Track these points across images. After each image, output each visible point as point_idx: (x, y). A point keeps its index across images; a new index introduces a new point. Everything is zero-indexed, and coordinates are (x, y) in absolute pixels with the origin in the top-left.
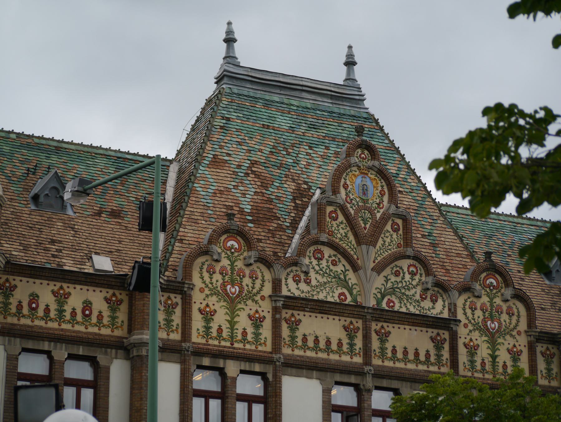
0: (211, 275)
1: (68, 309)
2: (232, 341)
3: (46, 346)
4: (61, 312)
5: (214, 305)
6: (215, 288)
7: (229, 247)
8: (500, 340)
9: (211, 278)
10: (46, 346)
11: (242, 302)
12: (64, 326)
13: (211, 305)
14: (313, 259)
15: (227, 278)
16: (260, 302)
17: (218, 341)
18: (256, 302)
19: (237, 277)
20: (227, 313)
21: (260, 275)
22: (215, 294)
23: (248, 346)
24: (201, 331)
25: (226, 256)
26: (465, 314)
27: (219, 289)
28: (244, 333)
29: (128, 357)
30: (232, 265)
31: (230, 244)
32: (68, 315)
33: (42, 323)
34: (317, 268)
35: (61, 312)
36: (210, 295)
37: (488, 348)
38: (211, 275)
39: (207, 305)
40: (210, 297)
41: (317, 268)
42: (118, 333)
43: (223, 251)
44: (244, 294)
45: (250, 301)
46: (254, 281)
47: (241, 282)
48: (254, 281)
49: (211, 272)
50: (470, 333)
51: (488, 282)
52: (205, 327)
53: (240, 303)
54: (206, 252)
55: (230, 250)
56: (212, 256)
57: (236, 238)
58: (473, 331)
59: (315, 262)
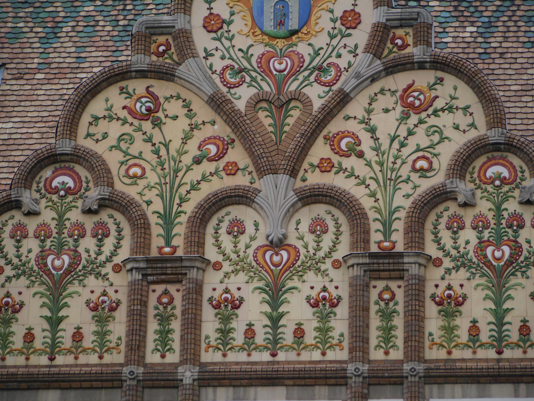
0: (18, 241)
2: (500, 345)
5: (239, 289)
6: (463, 256)
7: (491, 177)
8: (518, 279)
9: (18, 248)
11: (519, 274)
15: (486, 234)
16: (112, 276)
17: (470, 350)
18: (105, 277)
19: (507, 230)
22: (464, 265)
24: (212, 339)
25: (50, 204)
26: (438, 241)
27: (471, 254)
28: (78, 336)
30: (498, 209)
31: (491, 172)
32: (239, 338)
36: (454, 268)
37: (264, 301)
38: (455, 233)
39: (449, 288)
40: (233, 275)
43: (479, 187)
44: (522, 258)
45: (92, 278)
46: (100, 240)
47: (516, 237)
48: (100, 240)
50: (447, 276)
51: (489, 173)
52: (443, 328)
53: (513, 274)
55: (492, 183)
56: (456, 199)
57: (72, 169)
58: (454, 272)
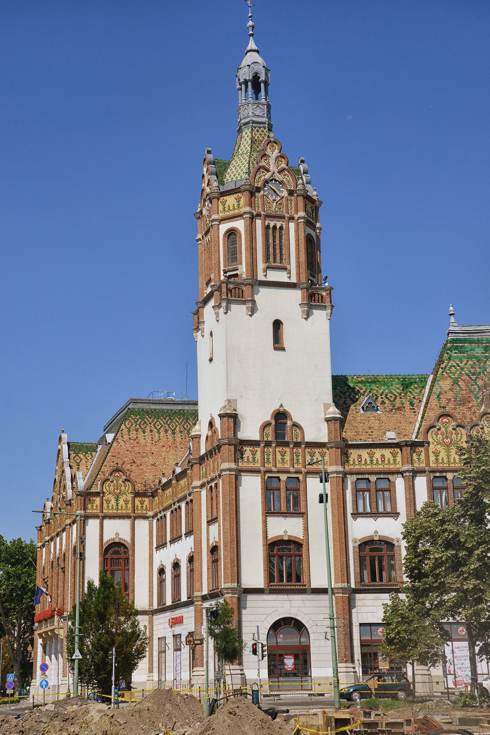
1: (374, 459)
3: (367, 476)
4: (372, 461)
10: (367, 476)
12: (374, 467)
13: (438, 449)
14: (485, 421)
20: (445, 452)
21: (460, 432)
23: (457, 465)
29: (403, 477)
33: (364, 467)
34: (488, 425)
35: (372, 461)
41: (488, 425)
42: (397, 466)
49: (437, 434)
54: (434, 427)
59: (486, 422)
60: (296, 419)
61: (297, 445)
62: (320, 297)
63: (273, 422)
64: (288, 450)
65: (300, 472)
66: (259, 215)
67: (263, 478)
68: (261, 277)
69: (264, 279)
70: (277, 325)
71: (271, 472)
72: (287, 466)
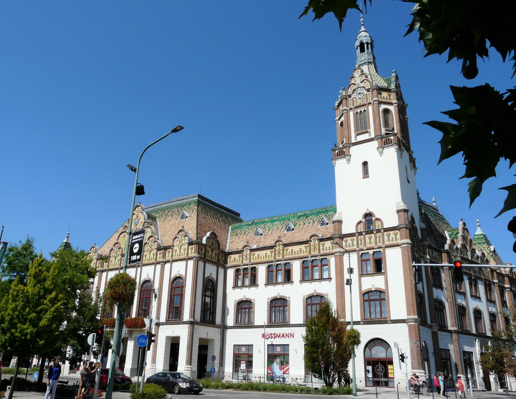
60: (377, 216)
61: (378, 231)
62: (390, 140)
63: (364, 220)
64: (373, 235)
65: (381, 248)
66: (351, 109)
67: (358, 254)
68: (353, 141)
69: (355, 141)
70: (365, 164)
71: (363, 250)
72: (373, 245)
